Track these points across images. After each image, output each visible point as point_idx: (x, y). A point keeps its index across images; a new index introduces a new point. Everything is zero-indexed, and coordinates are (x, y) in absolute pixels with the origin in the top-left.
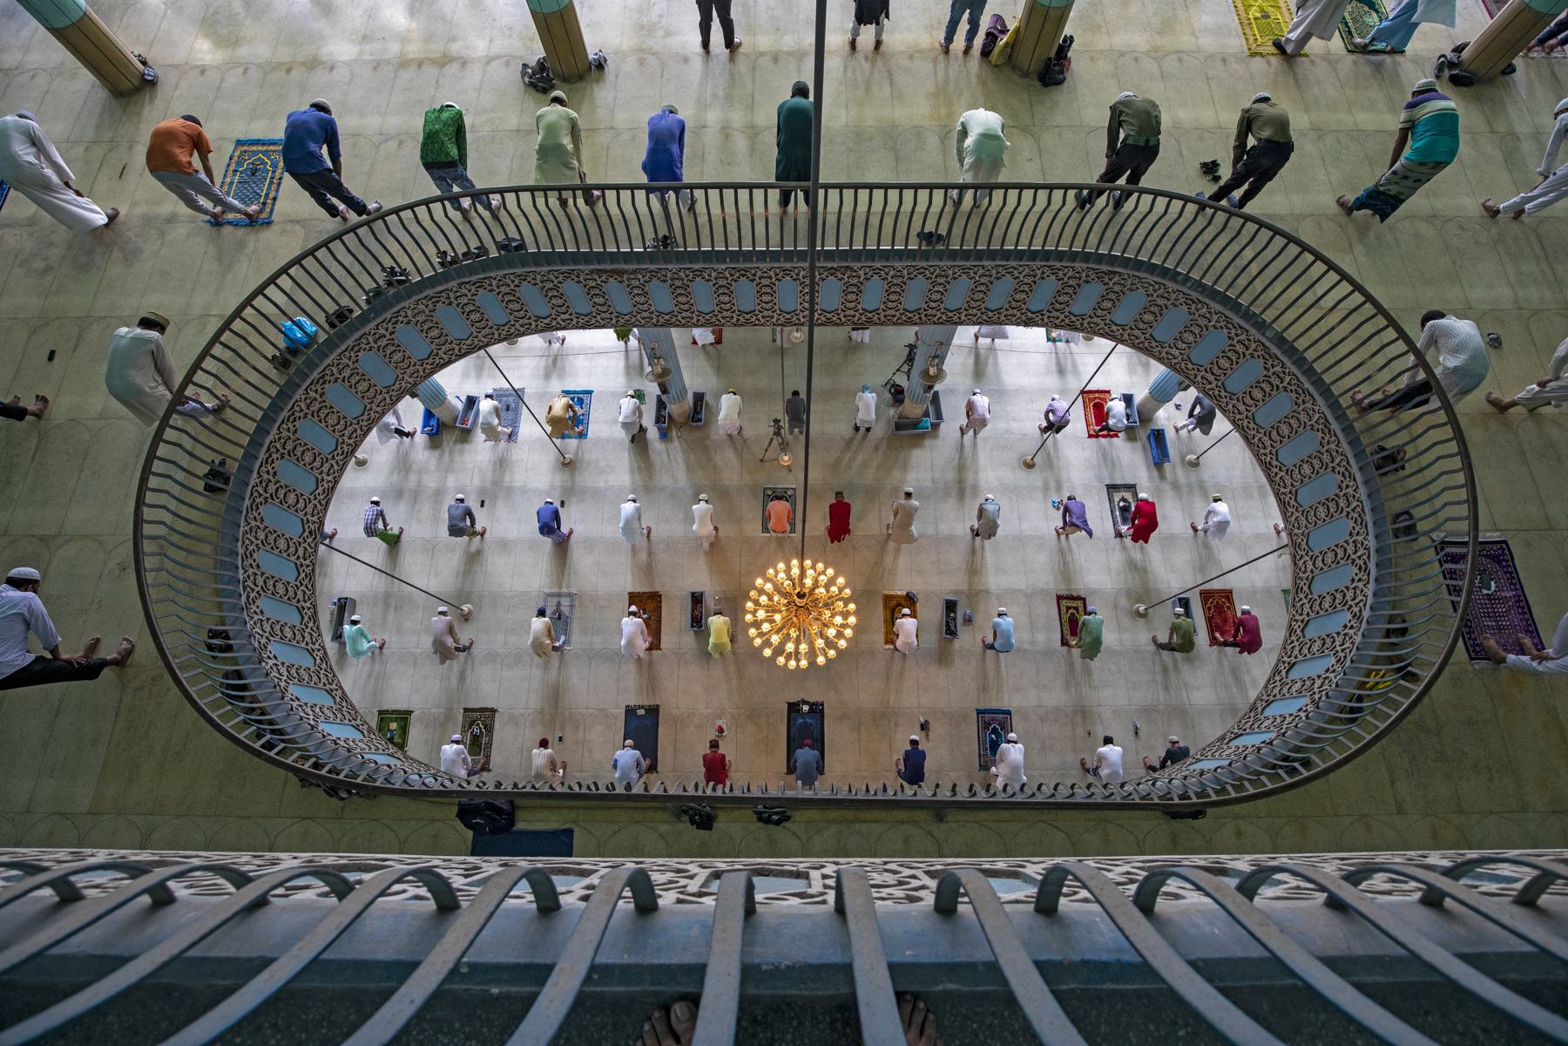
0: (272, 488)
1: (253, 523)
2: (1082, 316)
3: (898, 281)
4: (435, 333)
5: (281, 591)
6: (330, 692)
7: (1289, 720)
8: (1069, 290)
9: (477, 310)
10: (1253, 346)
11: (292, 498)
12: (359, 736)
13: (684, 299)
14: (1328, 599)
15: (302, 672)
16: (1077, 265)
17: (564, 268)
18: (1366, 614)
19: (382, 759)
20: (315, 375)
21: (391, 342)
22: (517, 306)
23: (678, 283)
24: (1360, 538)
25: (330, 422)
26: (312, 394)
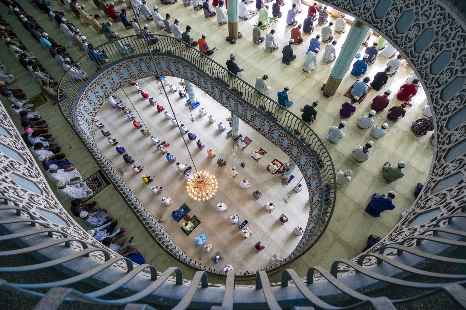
0: (118, 71)
9: (178, 68)
11: (121, 76)
12: (88, 118)
21: (159, 63)
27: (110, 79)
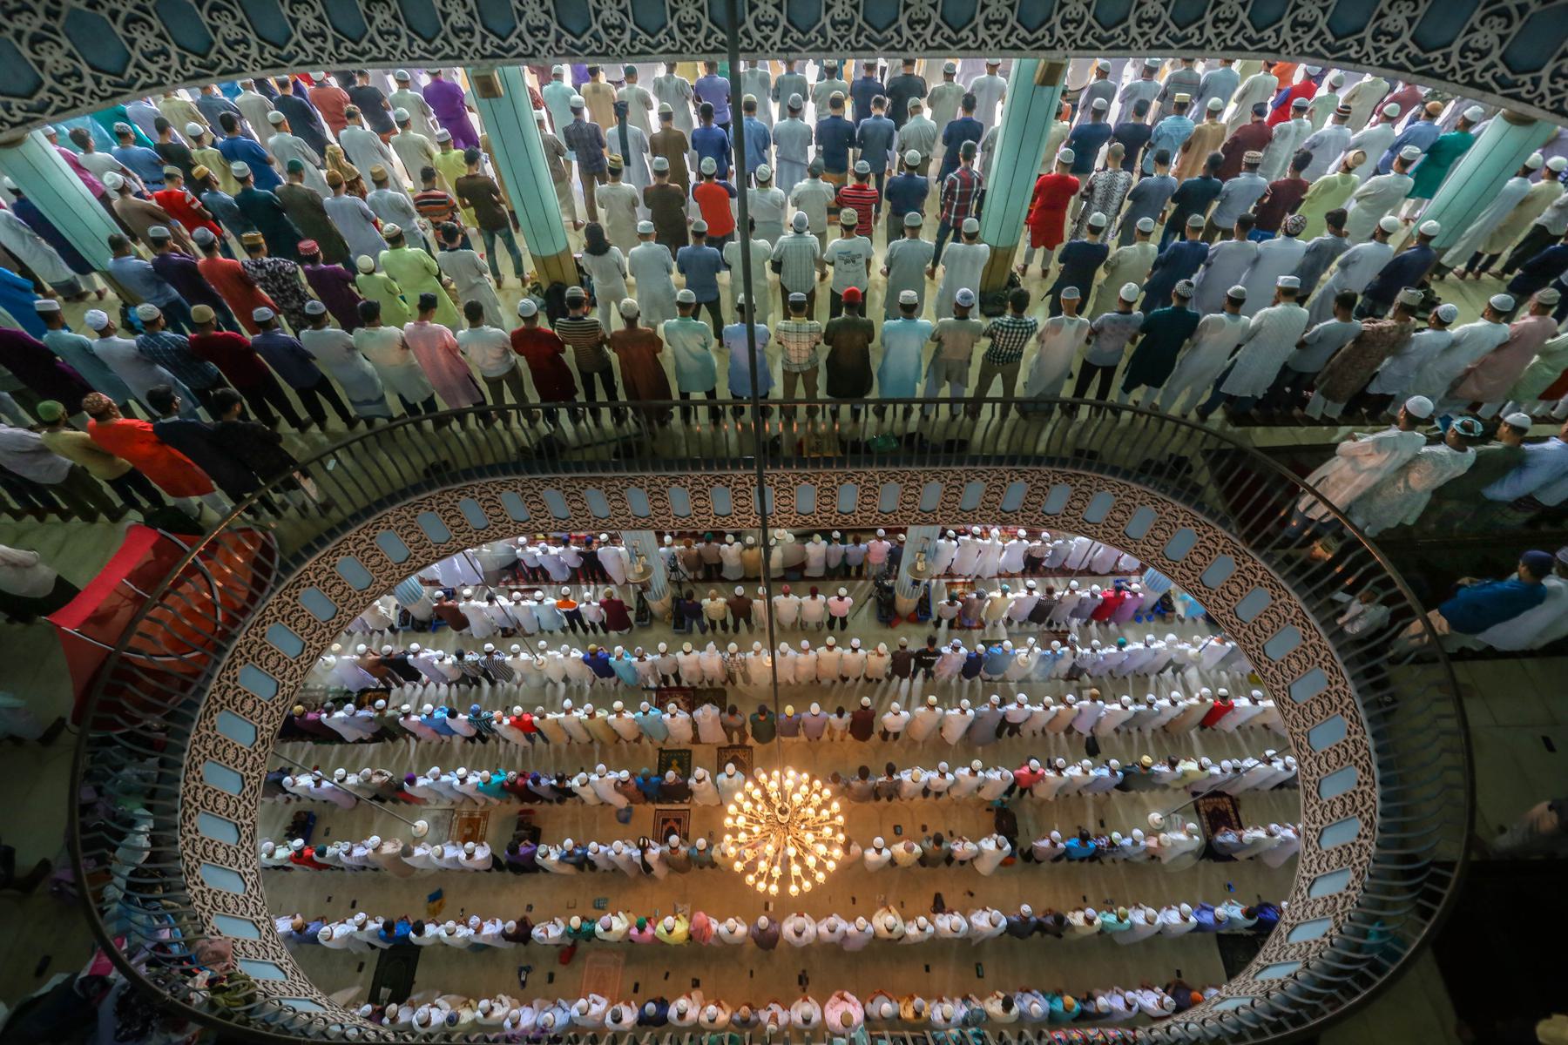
0: (230, 694)
1: (204, 732)
2: (1055, 515)
3: (871, 485)
4: (414, 537)
5: (221, 806)
6: (255, 924)
7: (1314, 947)
8: (1039, 491)
9: (458, 515)
10: (1222, 542)
12: (281, 977)
13: (660, 504)
14: (1338, 805)
15: (229, 900)
16: (1044, 469)
17: (544, 476)
18: (1377, 820)
19: (303, 1007)
20: (291, 579)
22: (497, 511)
23: (655, 489)
24: (1358, 737)
25: (300, 625)
26: (286, 598)
27: (220, 750)
